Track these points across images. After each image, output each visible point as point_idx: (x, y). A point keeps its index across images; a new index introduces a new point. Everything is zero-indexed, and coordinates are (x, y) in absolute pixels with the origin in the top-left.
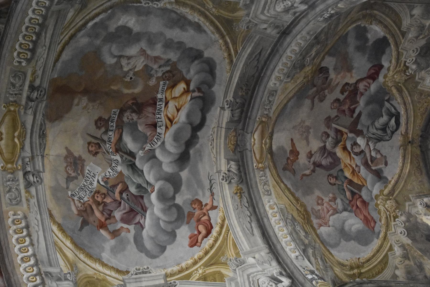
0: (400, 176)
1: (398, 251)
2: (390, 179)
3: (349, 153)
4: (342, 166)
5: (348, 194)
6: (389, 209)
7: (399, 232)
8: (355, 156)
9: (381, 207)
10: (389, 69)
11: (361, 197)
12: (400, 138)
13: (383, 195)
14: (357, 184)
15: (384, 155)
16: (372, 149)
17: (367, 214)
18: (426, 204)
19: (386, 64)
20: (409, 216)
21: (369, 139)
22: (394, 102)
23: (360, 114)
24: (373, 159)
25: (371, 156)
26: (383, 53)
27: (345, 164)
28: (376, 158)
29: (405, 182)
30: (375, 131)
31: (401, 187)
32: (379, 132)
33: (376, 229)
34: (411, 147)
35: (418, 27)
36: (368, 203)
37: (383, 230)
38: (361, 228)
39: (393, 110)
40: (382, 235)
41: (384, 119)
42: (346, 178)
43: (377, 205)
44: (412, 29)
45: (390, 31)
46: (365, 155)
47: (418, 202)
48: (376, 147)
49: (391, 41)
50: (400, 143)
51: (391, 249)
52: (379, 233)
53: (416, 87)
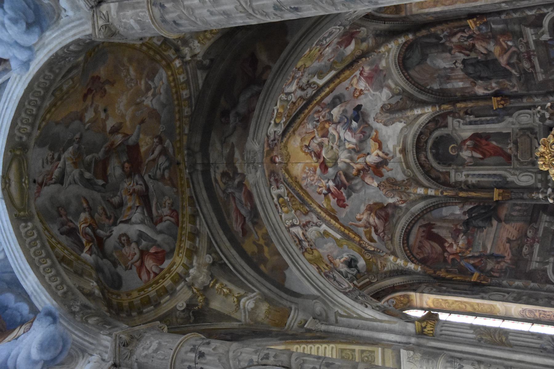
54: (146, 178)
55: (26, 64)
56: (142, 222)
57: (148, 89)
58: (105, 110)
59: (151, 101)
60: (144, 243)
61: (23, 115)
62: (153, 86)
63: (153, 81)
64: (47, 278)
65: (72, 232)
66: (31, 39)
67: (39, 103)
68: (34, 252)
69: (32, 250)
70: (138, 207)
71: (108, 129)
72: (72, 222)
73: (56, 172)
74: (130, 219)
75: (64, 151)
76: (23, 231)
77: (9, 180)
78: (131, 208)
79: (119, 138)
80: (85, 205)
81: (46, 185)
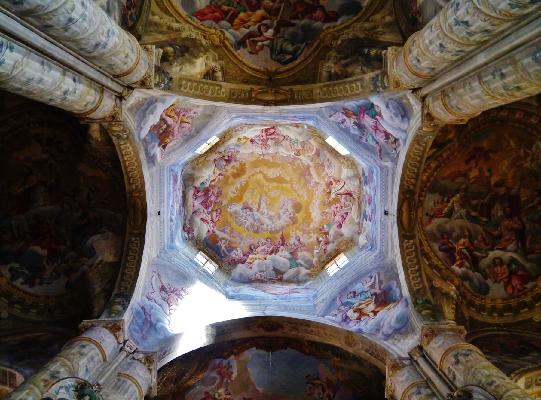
0: (241, 61)
1: (175, 25)
2: (239, 51)
3: (260, 22)
4: (249, 13)
5: (225, 8)
6: (212, 36)
7: (192, 34)
8: (257, 26)
9: (213, 31)
10: (335, 26)
11: (223, 19)
12: (274, 69)
13: (224, 39)
14: (234, 21)
15: (259, 53)
16: (264, 43)
17: (208, 16)
18: (216, 72)
19: (339, 22)
20: (206, 50)
21: (272, 40)
22: (306, 49)
23: (294, 25)
24: (255, 42)
25: (257, 41)
26: (348, 14)
27: (251, 16)
28: (256, 45)
29: (235, 64)
30: (279, 44)
31: (232, 58)
32: (278, 48)
33: (194, 18)
34: (266, 79)
35: (375, 26)
36: (217, 23)
37: (194, 23)
38: (196, 6)
39: (299, 52)
40: (189, 19)
41: (290, 48)
42: (239, 13)
43: (216, 29)
44: (373, 23)
45: (369, 9)
46: (259, 36)
47: (219, 67)
48: (265, 47)
49: (360, 14)
50: (269, 68)
51: (177, 21)
52: (191, 19)
53: (321, 59)
54: (524, 219)
55: (405, 141)
56: (515, 251)
57: (527, 155)
58: (489, 170)
59: (531, 164)
60: (514, 266)
61: (408, 173)
62: (531, 153)
63: (531, 149)
64: (411, 277)
65: (449, 252)
66: (404, 126)
67: (418, 165)
68: (409, 259)
69: (408, 258)
70: (513, 240)
71: (493, 183)
72: (451, 243)
73: (446, 210)
74: (506, 248)
75: (453, 196)
76: (405, 245)
77: (402, 212)
78: (507, 240)
79: (502, 190)
80: (467, 233)
81: (436, 217)
